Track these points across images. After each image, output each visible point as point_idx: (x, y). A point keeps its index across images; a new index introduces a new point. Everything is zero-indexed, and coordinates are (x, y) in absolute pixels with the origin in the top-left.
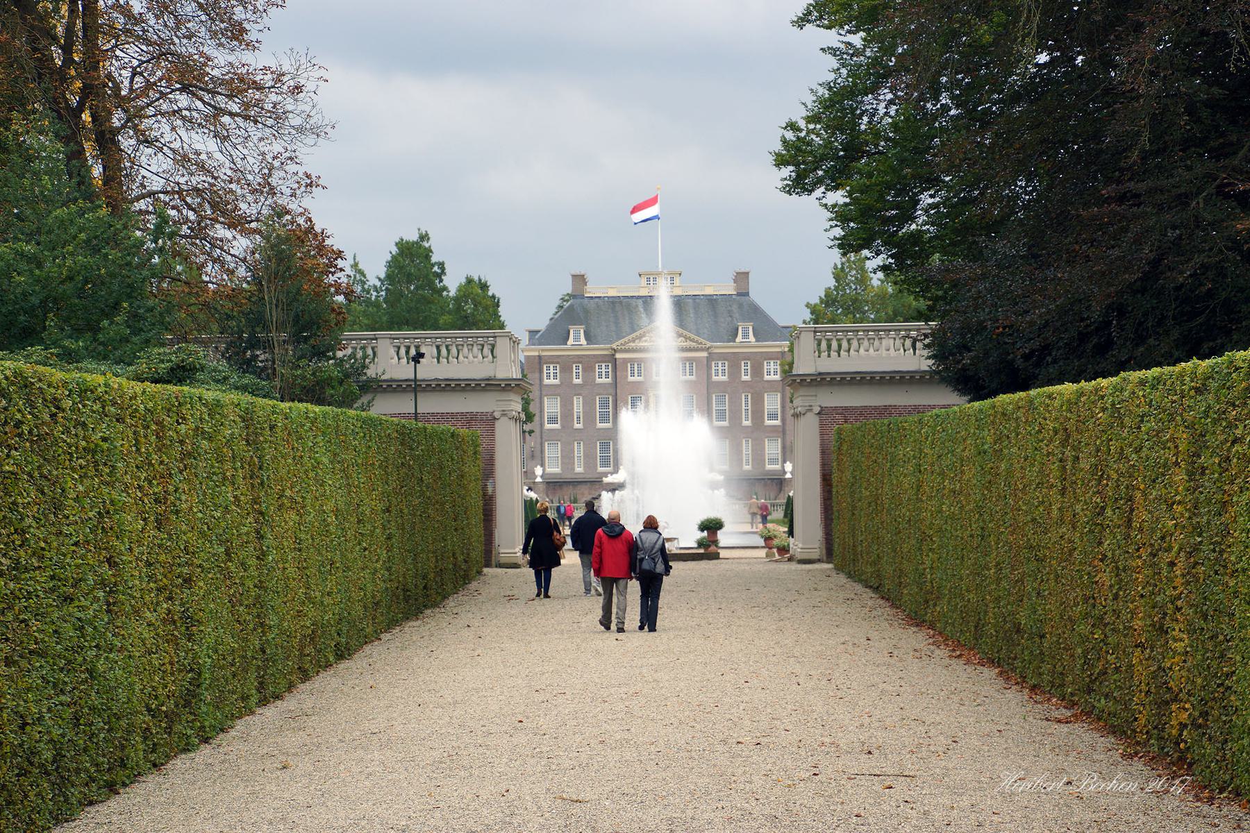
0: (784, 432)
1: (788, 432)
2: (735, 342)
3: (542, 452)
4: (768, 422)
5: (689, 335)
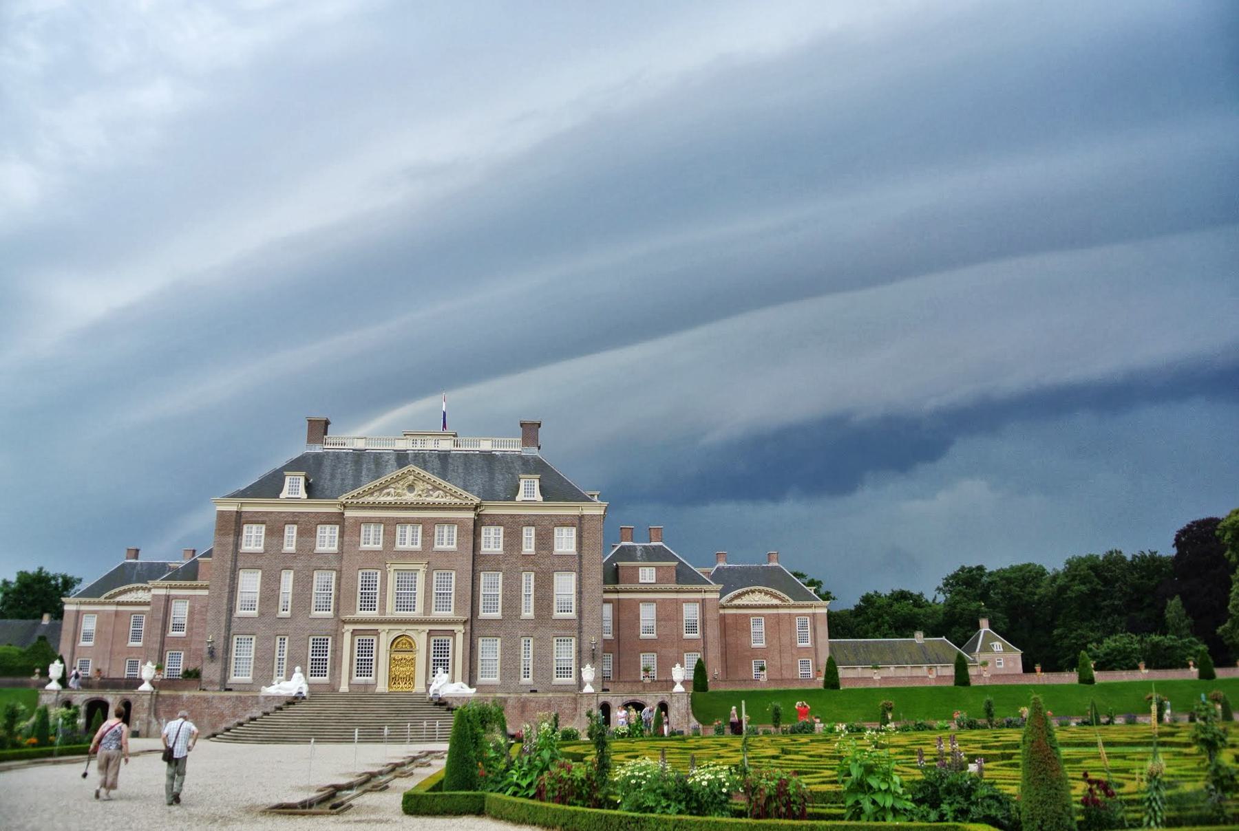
0: (580, 628)
1: (585, 629)
3: (227, 650)
4: (557, 615)
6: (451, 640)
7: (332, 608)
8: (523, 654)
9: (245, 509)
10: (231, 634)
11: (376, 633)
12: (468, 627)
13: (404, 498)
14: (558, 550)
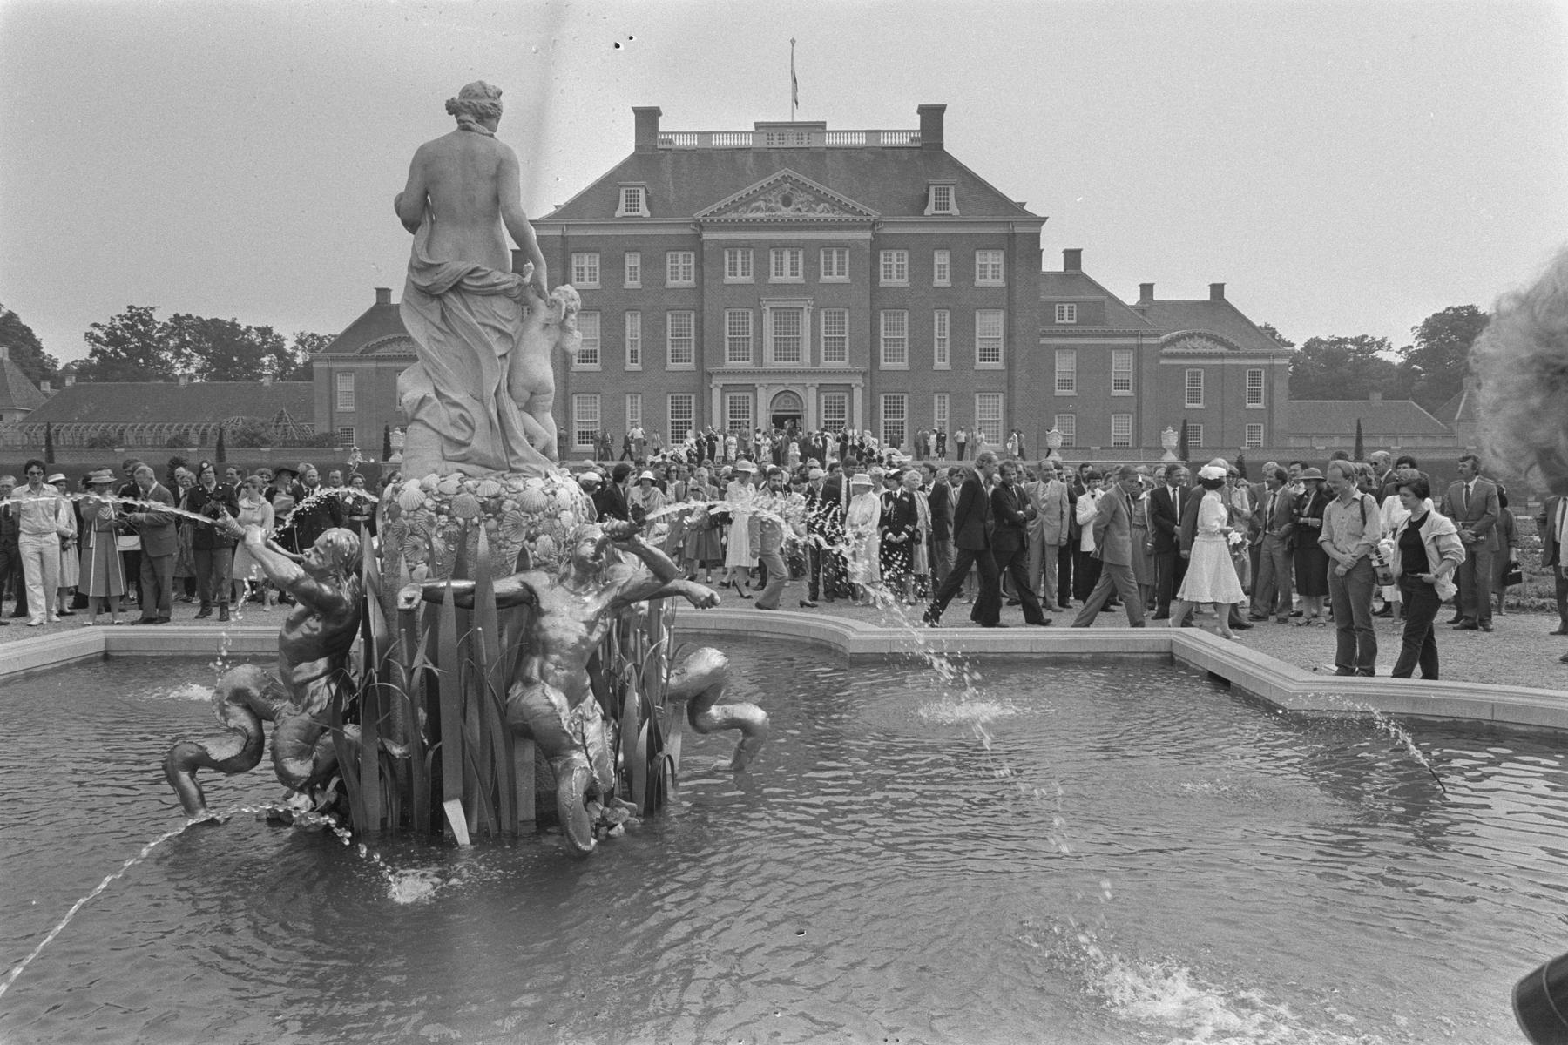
2: (922, 214)
5: (838, 196)
6: (847, 399)
7: (693, 359)
8: (936, 413)
9: (573, 233)
10: (570, 390)
11: (753, 388)
12: (868, 381)
13: (779, 213)
14: (979, 282)
